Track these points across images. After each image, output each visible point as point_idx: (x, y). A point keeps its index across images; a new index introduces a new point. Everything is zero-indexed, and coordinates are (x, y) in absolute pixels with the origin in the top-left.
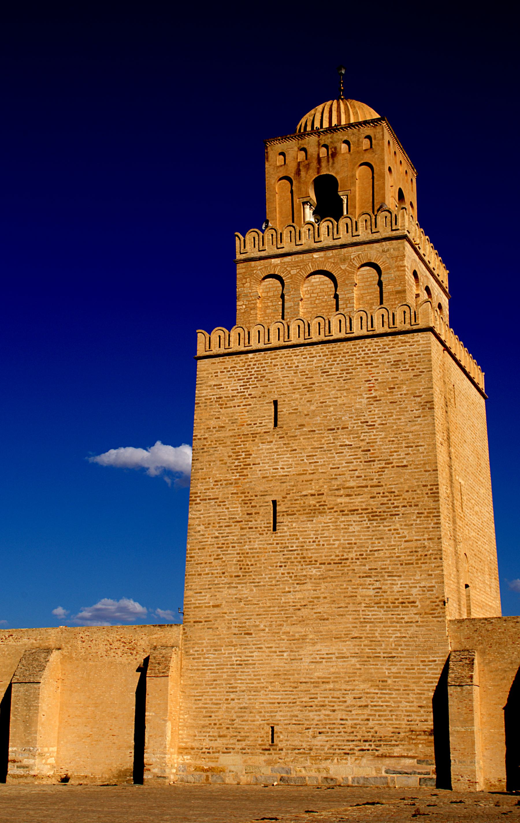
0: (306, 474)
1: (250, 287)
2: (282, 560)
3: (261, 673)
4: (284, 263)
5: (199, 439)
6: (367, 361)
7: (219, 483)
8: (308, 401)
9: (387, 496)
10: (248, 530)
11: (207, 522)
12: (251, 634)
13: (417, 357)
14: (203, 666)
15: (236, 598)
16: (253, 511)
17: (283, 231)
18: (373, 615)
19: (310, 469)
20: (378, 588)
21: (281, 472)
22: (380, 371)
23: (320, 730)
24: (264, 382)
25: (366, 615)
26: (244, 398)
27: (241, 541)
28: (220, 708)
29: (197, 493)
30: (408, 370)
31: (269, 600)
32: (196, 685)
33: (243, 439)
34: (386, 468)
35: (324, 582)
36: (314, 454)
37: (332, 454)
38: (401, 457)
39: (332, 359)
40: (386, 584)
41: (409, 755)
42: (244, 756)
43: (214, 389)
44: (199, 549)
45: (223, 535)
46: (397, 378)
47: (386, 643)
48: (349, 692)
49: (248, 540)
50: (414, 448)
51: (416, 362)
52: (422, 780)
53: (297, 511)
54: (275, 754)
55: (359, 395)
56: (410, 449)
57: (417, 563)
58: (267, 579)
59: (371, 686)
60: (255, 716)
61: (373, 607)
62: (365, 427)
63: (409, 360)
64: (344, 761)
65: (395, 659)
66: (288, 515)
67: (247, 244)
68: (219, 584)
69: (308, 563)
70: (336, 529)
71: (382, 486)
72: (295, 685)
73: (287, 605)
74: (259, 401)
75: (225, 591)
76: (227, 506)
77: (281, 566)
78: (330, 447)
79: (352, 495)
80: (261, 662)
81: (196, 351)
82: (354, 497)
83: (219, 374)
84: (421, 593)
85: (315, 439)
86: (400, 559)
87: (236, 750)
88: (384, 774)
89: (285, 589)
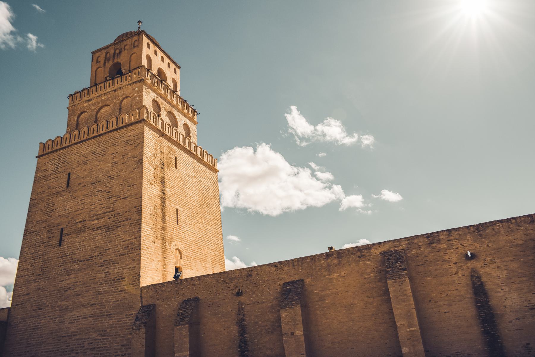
59: (98, 335)
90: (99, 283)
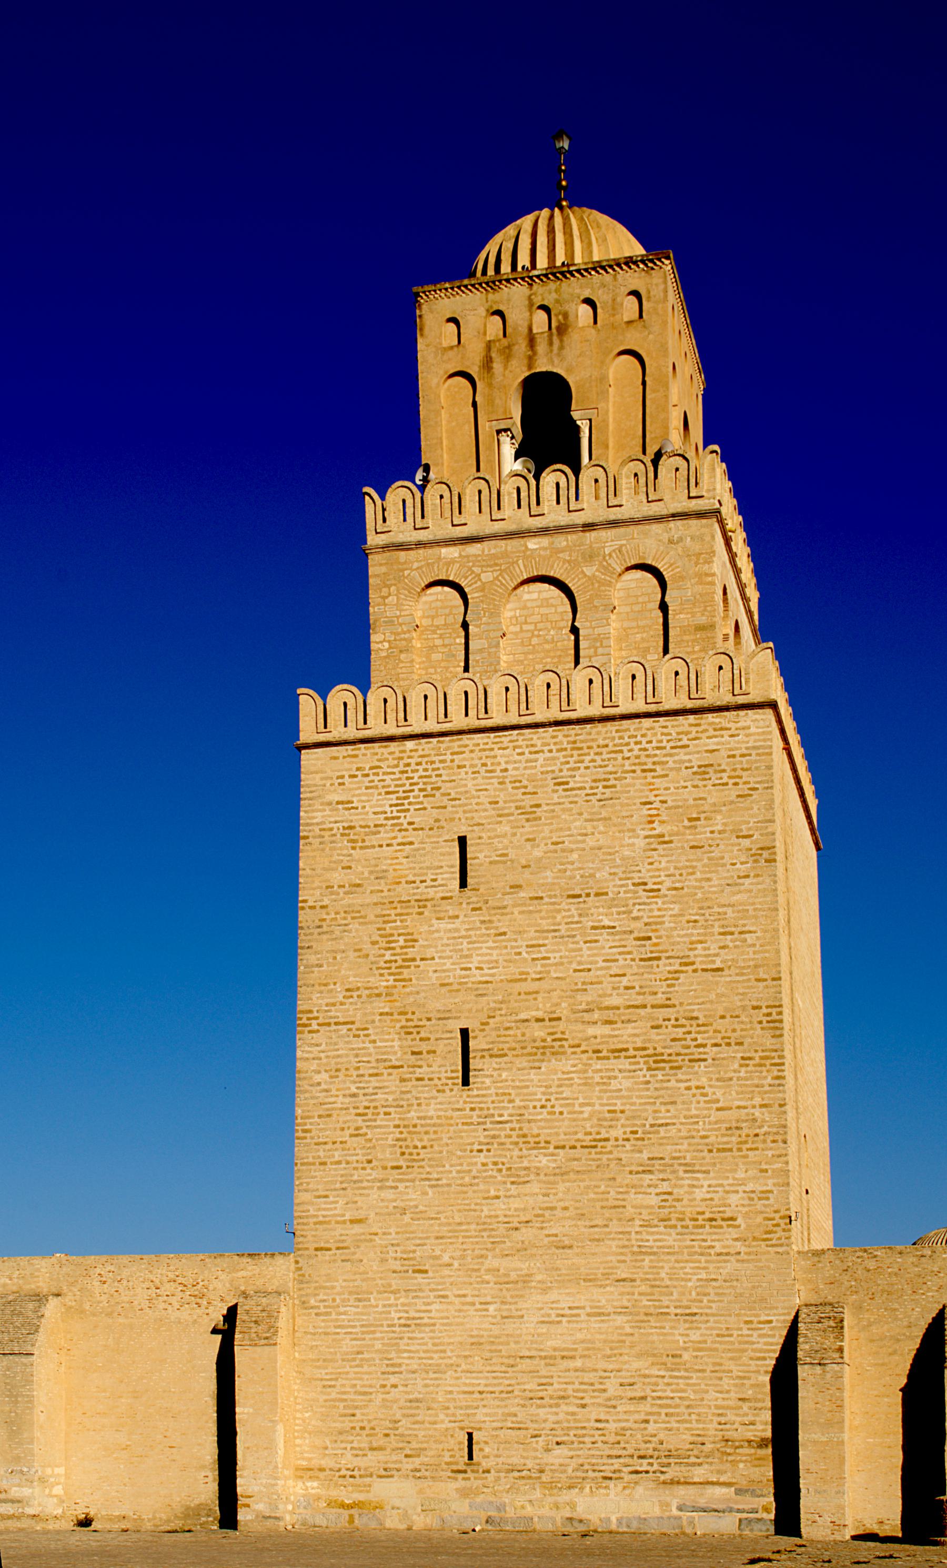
0: (526, 979)
1: (398, 605)
2: (482, 1139)
3: (446, 1340)
4: (468, 556)
5: (311, 907)
6: (645, 764)
7: (355, 994)
8: (528, 840)
9: (683, 1026)
10: (415, 1083)
11: (334, 1067)
12: (426, 1272)
13: (744, 759)
14: (335, 1327)
15: (395, 1207)
16: (424, 1047)
17: (464, 488)
18: (655, 1241)
19: (533, 970)
20: (665, 1193)
21: (477, 976)
22: (671, 785)
23: (559, 1439)
24: (438, 799)
25: (642, 1240)
26: (400, 831)
27: (402, 1103)
28: (370, 1401)
29: (311, 1012)
30: (727, 784)
31: (459, 1211)
32: (324, 1360)
33: (399, 911)
34: (682, 972)
35: (563, 1181)
36: (541, 942)
37: (577, 943)
38: (712, 952)
39: (576, 758)
40: (682, 1186)
41: (722, 1480)
42: (418, 1482)
43: (337, 809)
44: (320, 1116)
45: (366, 1091)
46: (704, 799)
47: (680, 1289)
48: (612, 1375)
49: (415, 1102)
50: (736, 936)
51: (742, 769)
52: (744, 1522)
53: (509, 1049)
54: (475, 1478)
55: (629, 830)
56: (729, 937)
57: (740, 1150)
58: (454, 1174)
60: (437, 1415)
61: (657, 1226)
62: (642, 893)
63: (728, 764)
64: (602, 1491)
65: (697, 1318)
66: (491, 1056)
67: (388, 515)
68: (361, 1181)
69: (532, 1145)
70: (585, 1084)
71: (674, 1006)
72: (511, 1361)
73: (494, 1220)
74: (429, 836)
75: (374, 1194)
76: (373, 1037)
77: (480, 1151)
78: (573, 929)
79: (616, 1023)
80: (445, 1321)
81: (298, 731)
82: (619, 1025)
83: (347, 780)
84: (746, 1202)
85: (543, 914)
86: (707, 1141)
87: (403, 1472)
88: (675, 1512)
89: (489, 1191)
90: (638, 1222)
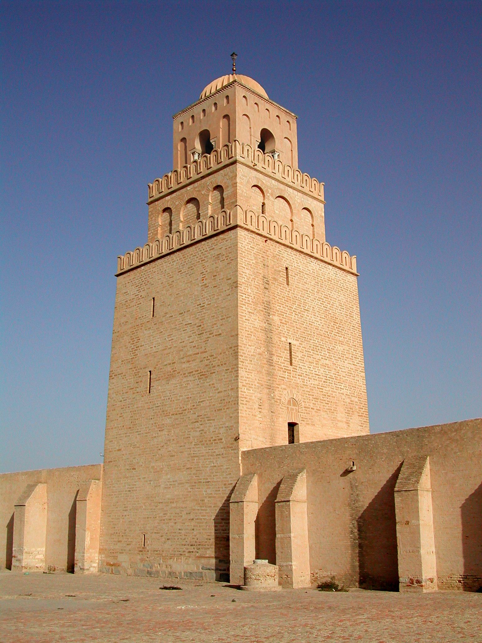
90: (193, 443)
